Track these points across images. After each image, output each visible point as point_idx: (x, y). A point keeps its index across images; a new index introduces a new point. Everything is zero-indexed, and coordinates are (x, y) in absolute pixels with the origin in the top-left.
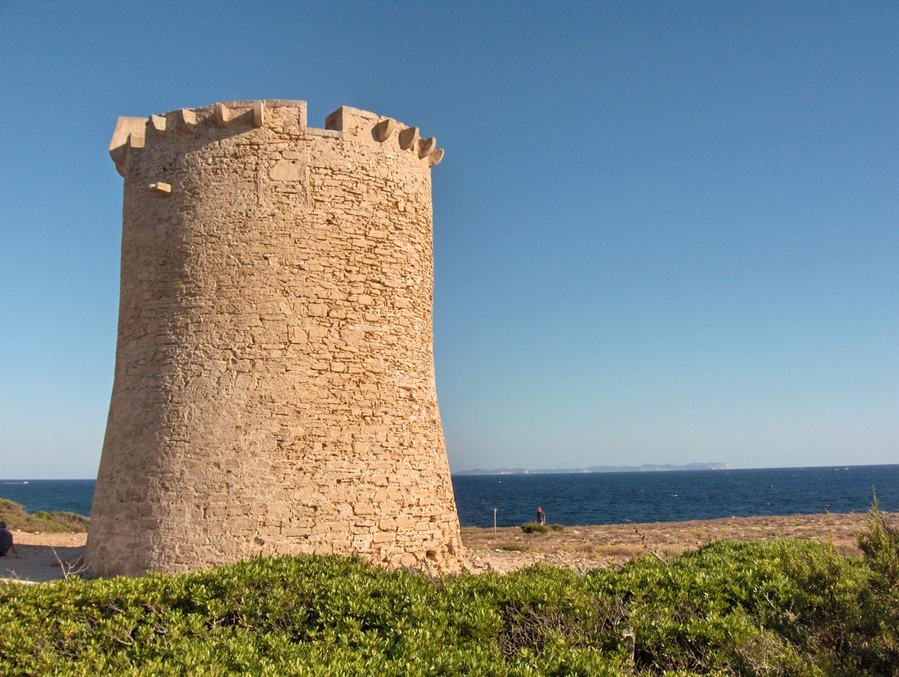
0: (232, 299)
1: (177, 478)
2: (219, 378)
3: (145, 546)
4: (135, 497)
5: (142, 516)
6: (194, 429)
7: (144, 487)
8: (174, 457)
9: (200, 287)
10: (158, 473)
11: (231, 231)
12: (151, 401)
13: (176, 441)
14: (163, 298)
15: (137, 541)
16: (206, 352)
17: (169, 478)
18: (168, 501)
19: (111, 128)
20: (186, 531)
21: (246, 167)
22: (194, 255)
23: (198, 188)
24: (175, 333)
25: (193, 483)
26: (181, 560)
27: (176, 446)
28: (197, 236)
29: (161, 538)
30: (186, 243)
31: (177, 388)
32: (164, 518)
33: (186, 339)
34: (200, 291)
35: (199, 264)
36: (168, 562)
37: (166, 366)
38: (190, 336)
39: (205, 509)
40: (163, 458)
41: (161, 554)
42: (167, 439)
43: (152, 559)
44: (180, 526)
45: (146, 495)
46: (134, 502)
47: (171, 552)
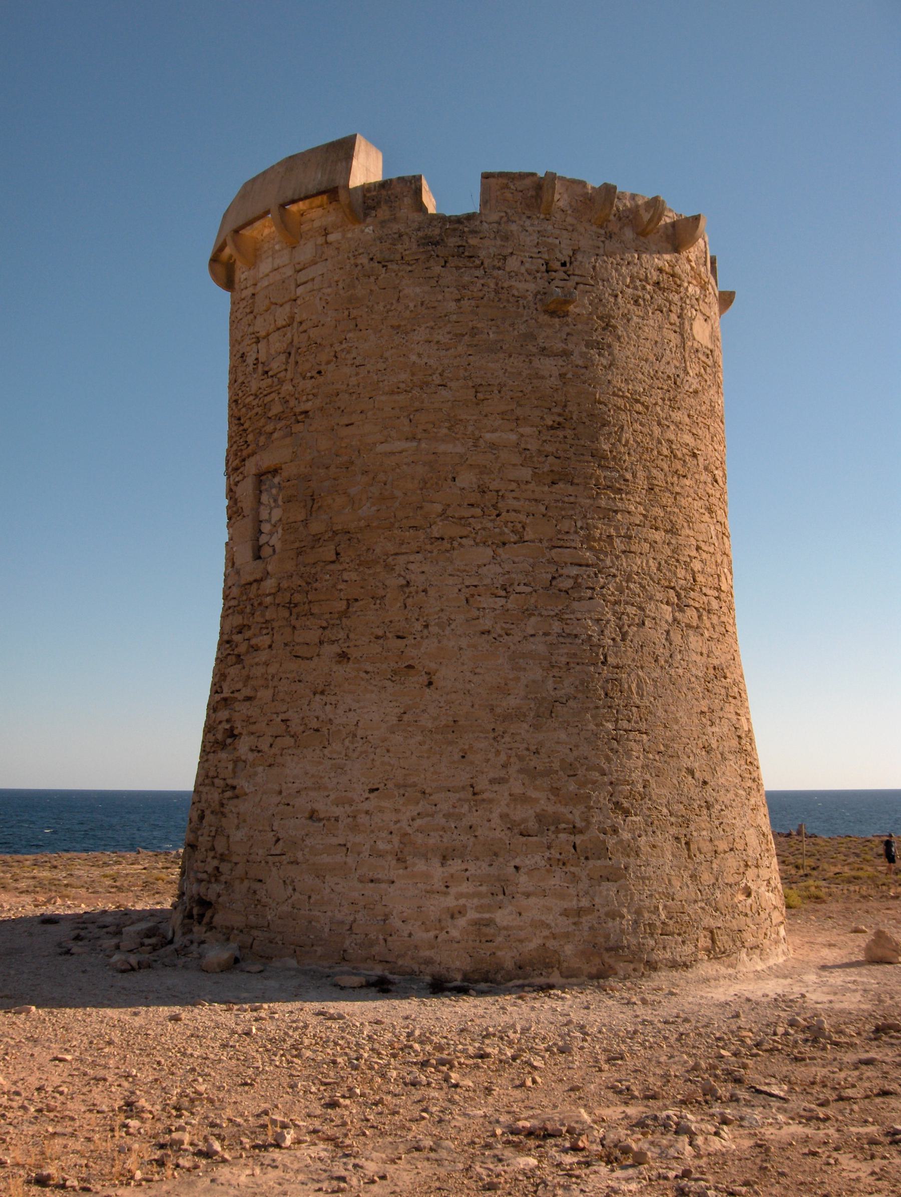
0: (669, 509)
1: (639, 793)
2: (668, 632)
3: (603, 911)
4: (563, 826)
5: (587, 858)
6: (650, 712)
7: (582, 808)
8: (629, 758)
9: (627, 480)
10: (605, 783)
11: (660, 402)
12: (564, 660)
13: (625, 731)
14: (561, 485)
15: (585, 903)
16: (644, 587)
17: (626, 793)
18: (632, 831)
19: (376, 142)
20: (669, 880)
21: (672, 308)
22: (614, 426)
23: (613, 318)
24: (591, 548)
25: (664, 801)
26: (670, 929)
27: (628, 739)
28: (618, 396)
29: (632, 894)
30: (600, 403)
31: (610, 642)
32: (632, 860)
33: (612, 561)
34: (628, 486)
35: (623, 442)
36: (652, 935)
37: (583, 602)
38: (617, 557)
39: (687, 843)
40: (608, 760)
41: (636, 922)
42: (610, 726)
43: (622, 931)
44: (659, 872)
45: (588, 823)
46: (562, 836)
47: (654, 917)
